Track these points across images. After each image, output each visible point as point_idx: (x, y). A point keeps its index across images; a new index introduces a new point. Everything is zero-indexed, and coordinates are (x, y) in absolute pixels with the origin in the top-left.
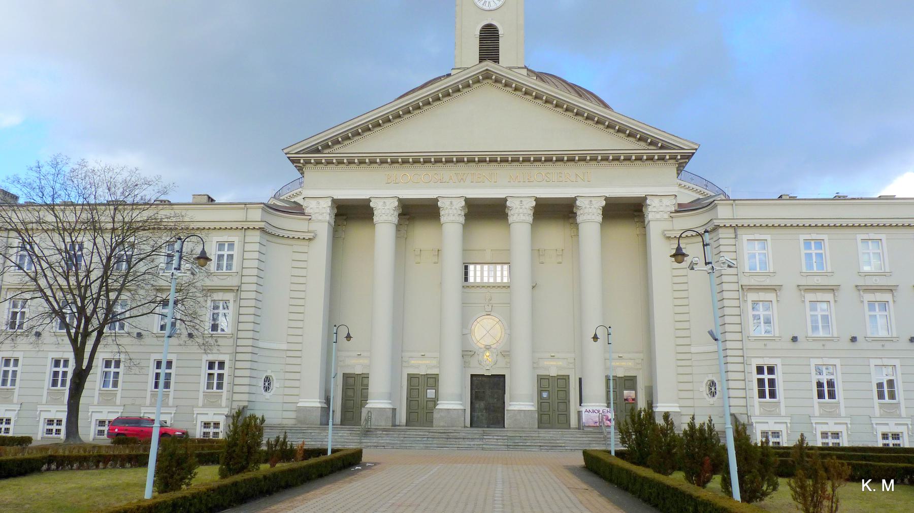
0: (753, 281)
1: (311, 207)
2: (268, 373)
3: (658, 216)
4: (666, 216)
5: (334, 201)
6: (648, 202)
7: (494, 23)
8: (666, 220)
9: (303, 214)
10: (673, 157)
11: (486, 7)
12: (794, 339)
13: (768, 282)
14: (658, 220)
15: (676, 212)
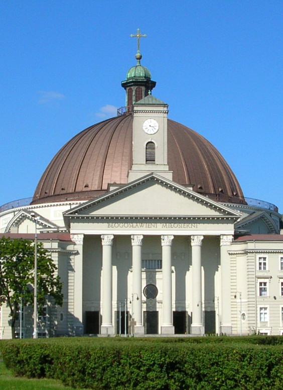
0: (260, 274)
1: (74, 238)
2: (62, 312)
3: (225, 244)
4: (229, 244)
5: (85, 235)
6: (221, 237)
7: (152, 141)
8: (228, 245)
9: (71, 241)
10: (233, 218)
11: (149, 133)
12: (275, 298)
13: (266, 274)
14: (225, 245)
15: (233, 242)
